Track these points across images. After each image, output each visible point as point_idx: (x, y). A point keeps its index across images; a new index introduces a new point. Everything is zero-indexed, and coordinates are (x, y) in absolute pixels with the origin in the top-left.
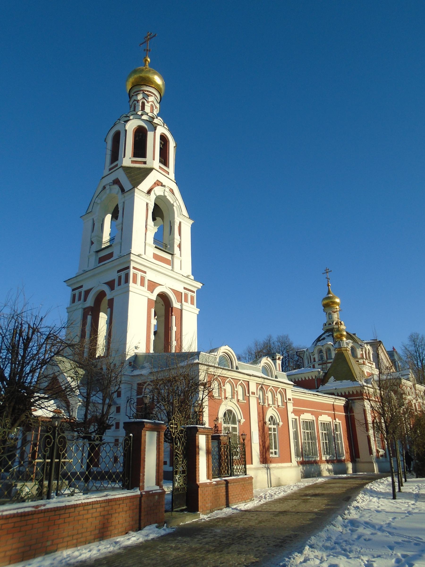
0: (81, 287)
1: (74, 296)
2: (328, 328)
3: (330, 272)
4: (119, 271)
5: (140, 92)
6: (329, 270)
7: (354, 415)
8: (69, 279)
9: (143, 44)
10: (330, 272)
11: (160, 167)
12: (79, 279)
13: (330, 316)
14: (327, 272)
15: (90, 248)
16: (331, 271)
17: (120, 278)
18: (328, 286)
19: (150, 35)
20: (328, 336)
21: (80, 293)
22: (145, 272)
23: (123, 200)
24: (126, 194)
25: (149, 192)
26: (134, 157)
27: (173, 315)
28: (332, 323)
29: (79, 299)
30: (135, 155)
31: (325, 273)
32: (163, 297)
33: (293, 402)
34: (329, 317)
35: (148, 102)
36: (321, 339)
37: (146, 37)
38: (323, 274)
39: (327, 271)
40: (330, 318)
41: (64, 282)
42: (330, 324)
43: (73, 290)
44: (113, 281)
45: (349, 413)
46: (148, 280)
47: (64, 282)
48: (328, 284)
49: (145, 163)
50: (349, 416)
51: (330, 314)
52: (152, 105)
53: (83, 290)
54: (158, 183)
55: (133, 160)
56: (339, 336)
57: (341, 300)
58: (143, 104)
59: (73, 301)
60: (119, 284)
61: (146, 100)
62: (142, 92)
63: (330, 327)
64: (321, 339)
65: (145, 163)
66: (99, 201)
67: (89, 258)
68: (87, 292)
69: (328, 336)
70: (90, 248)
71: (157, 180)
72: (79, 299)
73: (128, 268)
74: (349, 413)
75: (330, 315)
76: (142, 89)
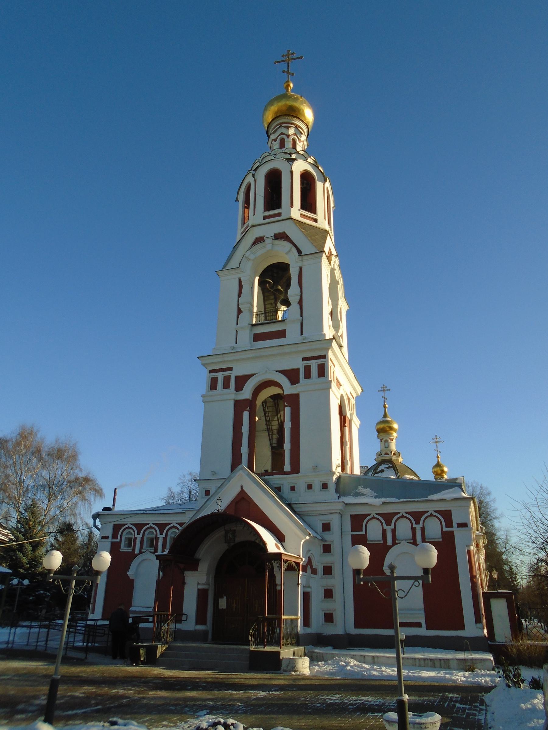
0: (230, 369)
2: (384, 459)
3: (387, 390)
4: (304, 359)
5: (292, 125)
6: (387, 389)
8: (208, 356)
9: (278, 62)
10: (387, 390)
12: (227, 358)
13: (386, 443)
14: (384, 391)
15: (238, 317)
16: (389, 390)
18: (385, 407)
19: (291, 54)
20: (388, 468)
23: (300, 264)
27: (346, 426)
28: (389, 453)
30: (303, 207)
31: (380, 391)
34: (385, 445)
35: (300, 141)
36: (378, 471)
37: (286, 56)
38: (379, 391)
39: (384, 389)
40: (387, 446)
42: (386, 454)
44: (297, 370)
47: (198, 357)
48: (385, 405)
49: (315, 221)
51: (386, 441)
53: (233, 375)
55: (303, 213)
56: (439, 472)
57: (399, 426)
58: (294, 141)
60: (308, 375)
61: (298, 138)
62: (294, 126)
63: (387, 457)
64: (378, 471)
66: (252, 257)
67: (237, 332)
69: (388, 468)
70: (238, 317)
73: (324, 357)
75: (386, 443)
76: (293, 122)
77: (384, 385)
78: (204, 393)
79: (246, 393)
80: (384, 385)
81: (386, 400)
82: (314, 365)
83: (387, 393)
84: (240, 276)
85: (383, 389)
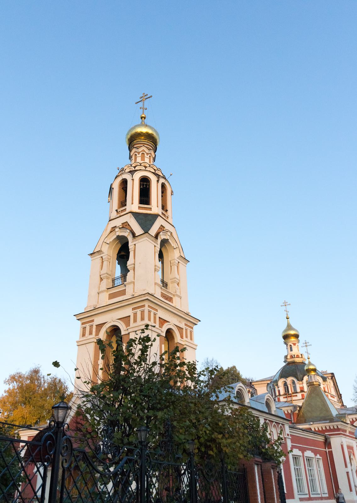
0: (93, 321)
1: (84, 328)
3: (288, 305)
4: (134, 309)
6: (288, 304)
7: (332, 451)
10: (288, 305)
11: (162, 213)
16: (290, 304)
17: (135, 315)
21: (91, 326)
22: (157, 310)
24: (137, 238)
25: (156, 237)
26: (140, 204)
29: (91, 333)
30: (141, 202)
32: (169, 332)
33: (291, 437)
41: (74, 315)
43: (83, 324)
45: (327, 448)
46: (159, 318)
47: (74, 315)
49: (150, 209)
50: (327, 452)
52: (150, 156)
54: (162, 228)
59: (84, 335)
60: (135, 321)
65: (150, 209)
68: (100, 326)
71: (161, 225)
72: (91, 333)
74: (327, 448)
77: (285, 301)
78: (78, 339)
79: (103, 336)
80: (285, 301)
81: (288, 313)
82: (139, 312)
83: (288, 307)
84: (101, 255)
85: (285, 304)
